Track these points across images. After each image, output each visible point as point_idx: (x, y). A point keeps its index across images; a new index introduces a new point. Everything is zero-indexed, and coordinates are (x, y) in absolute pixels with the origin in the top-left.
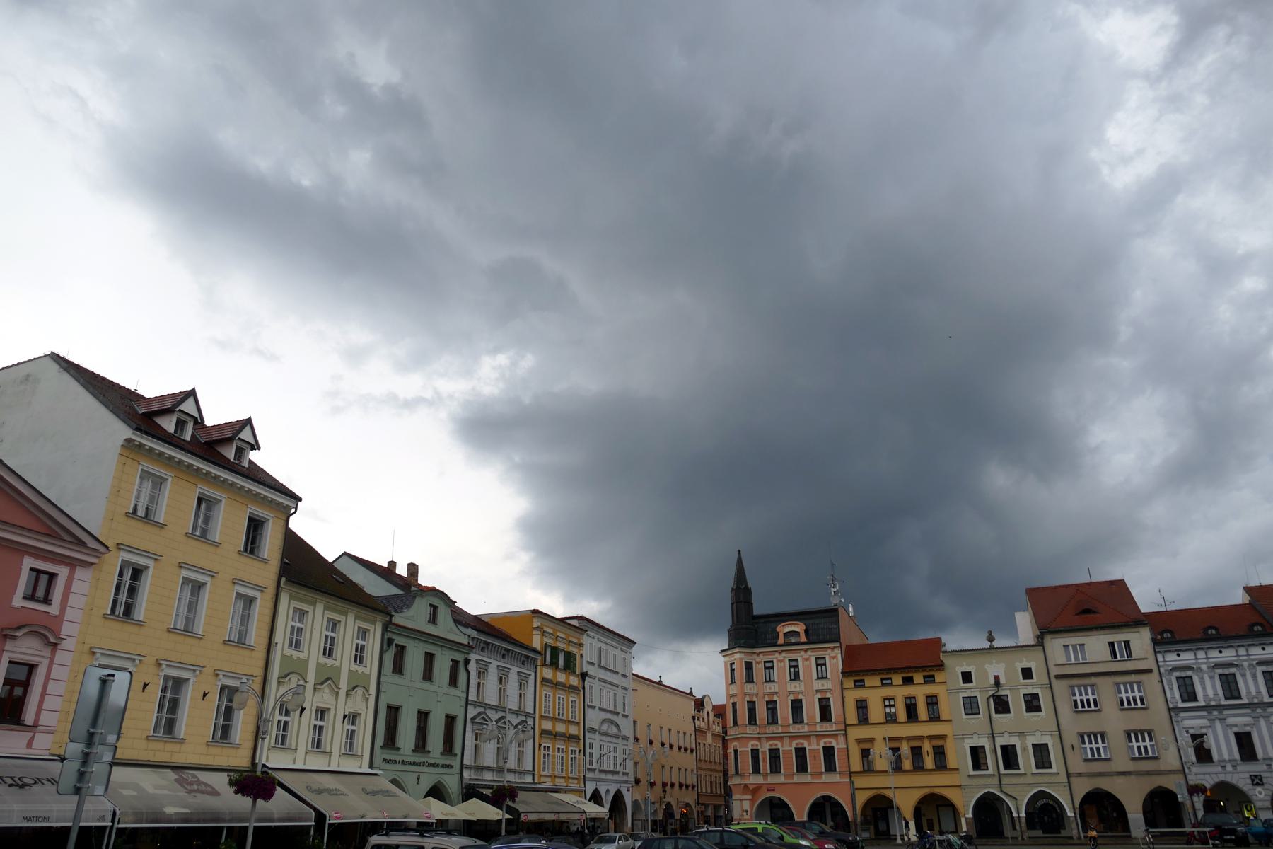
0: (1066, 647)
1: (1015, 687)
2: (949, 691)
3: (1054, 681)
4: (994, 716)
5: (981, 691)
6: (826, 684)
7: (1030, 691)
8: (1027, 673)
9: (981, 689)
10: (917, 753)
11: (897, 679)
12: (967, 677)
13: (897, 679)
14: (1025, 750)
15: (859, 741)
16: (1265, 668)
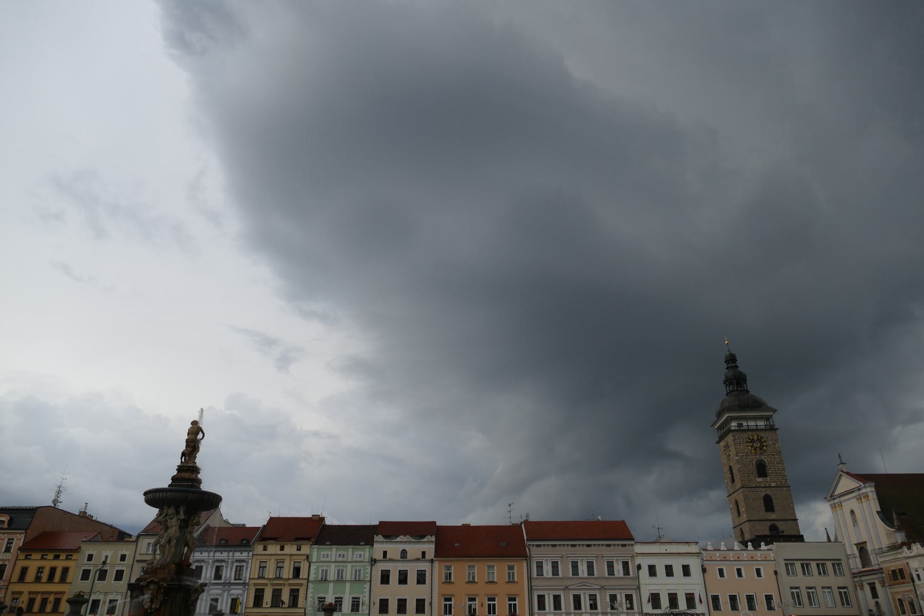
0: (149, 544)
1: (113, 566)
2: (77, 565)
3: (135, 563)
4: (96, 581)
5: (93, 567)
6: (8, 556)
7: (120, 568)
8: (123, 558)
9: (95, 565)
10: (44, 602)
11: (51, 556)
12: (90, 557)
13: (51, 556)
14: (104, 603)
15: (13, 593)
16: (237, 564)
